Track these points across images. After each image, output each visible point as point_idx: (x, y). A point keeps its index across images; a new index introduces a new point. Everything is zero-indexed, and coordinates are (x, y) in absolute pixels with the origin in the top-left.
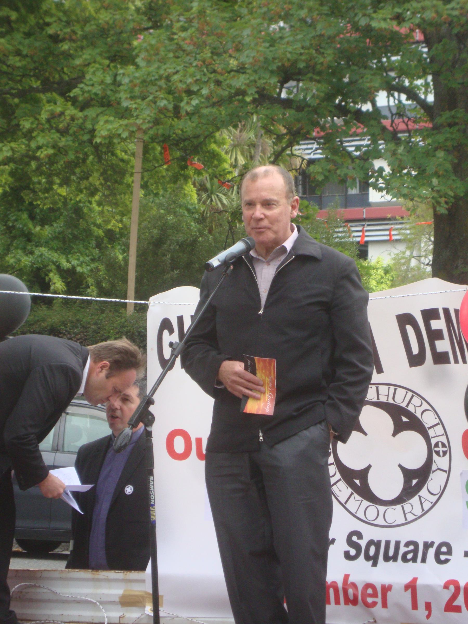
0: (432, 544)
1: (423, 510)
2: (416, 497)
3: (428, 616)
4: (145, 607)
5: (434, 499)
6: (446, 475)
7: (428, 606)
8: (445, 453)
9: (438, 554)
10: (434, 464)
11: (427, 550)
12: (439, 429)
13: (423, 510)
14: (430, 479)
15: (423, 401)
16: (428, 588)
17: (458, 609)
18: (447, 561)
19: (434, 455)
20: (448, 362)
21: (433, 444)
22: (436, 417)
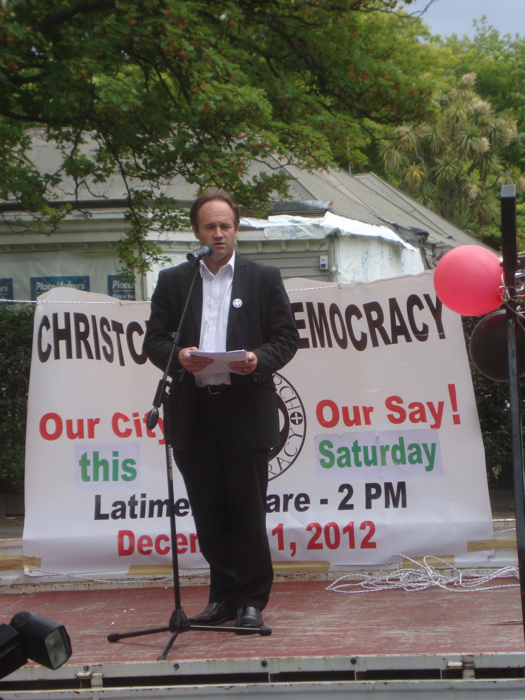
0: (291, 496)
1: (281, 469)
2: (275, 459)
3: (293, 555)
4: (23, 569)
5: (291, 459)
6: (301, 439)
7: (293, 546)
8: (300, 422)
9: (297, 503)
10: (290, 431)
11: (288, 502)
12: (296, 402)
13: (281, 469)
14: (287, 443)
15: (282, 380)
16: (293, 531)
17: (320, 546)
18: (306, 508)
19: (291, 423)
20: (308, 346)
21: (290, 415)
22: (294, 392)
